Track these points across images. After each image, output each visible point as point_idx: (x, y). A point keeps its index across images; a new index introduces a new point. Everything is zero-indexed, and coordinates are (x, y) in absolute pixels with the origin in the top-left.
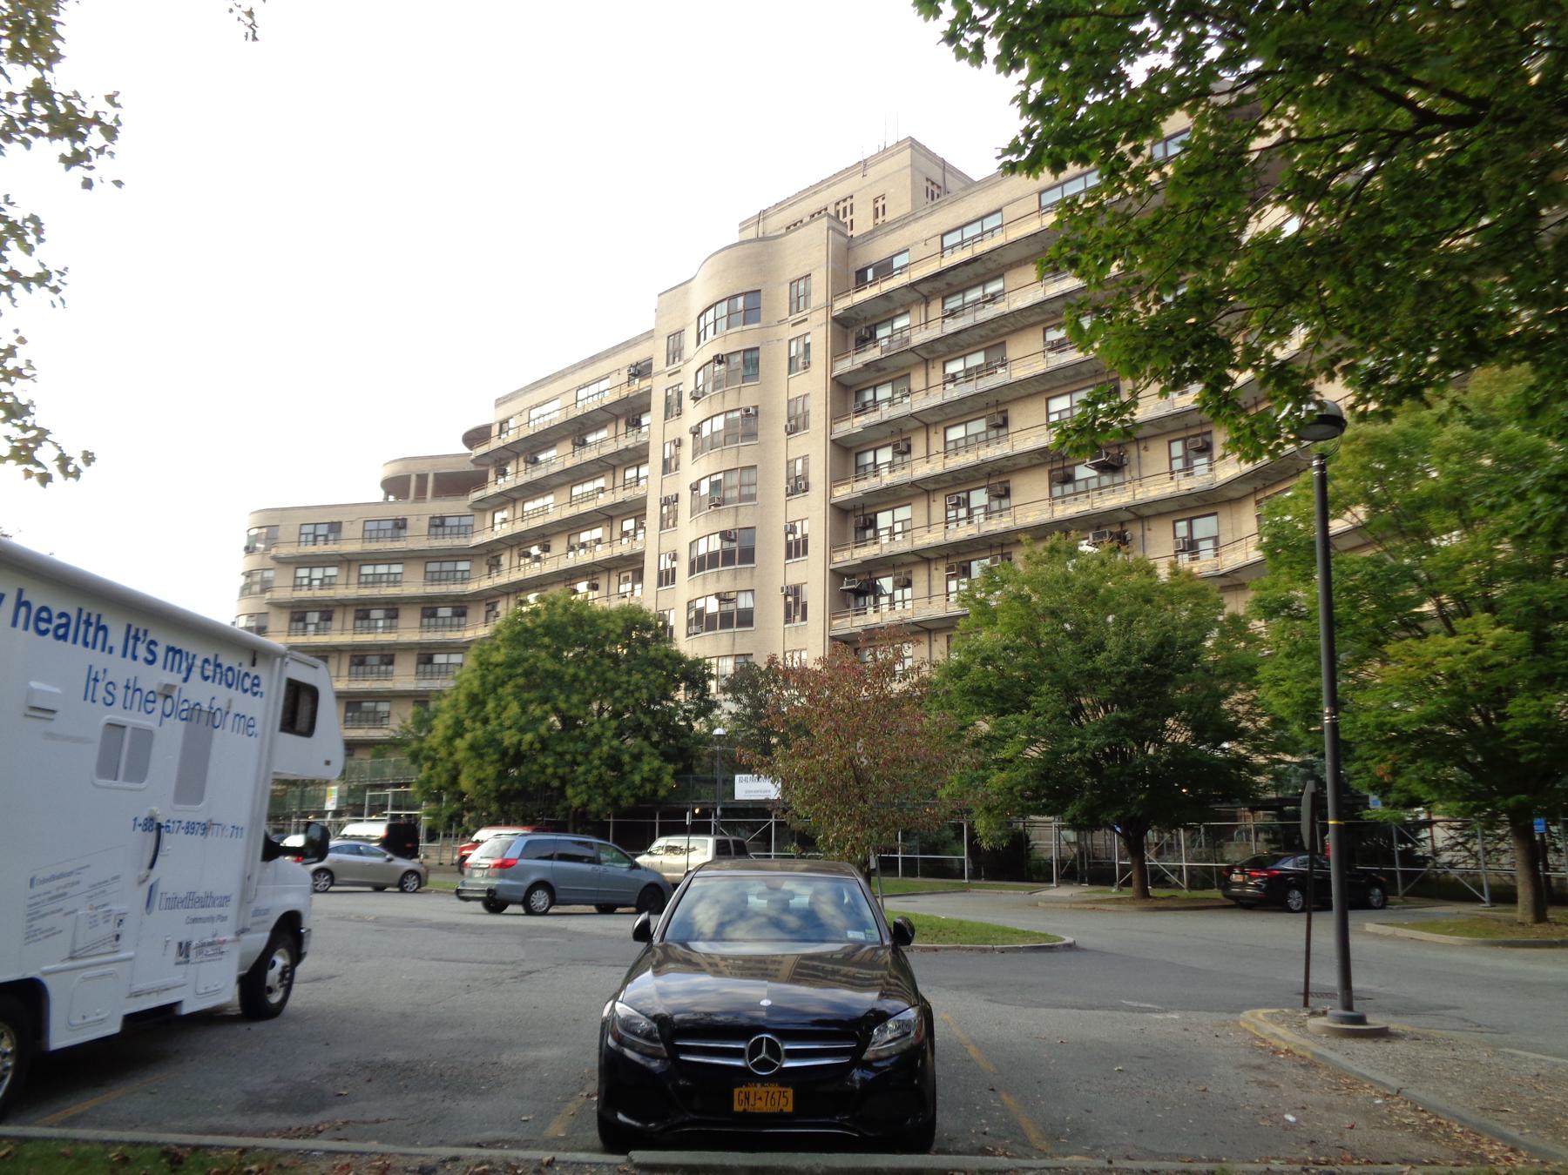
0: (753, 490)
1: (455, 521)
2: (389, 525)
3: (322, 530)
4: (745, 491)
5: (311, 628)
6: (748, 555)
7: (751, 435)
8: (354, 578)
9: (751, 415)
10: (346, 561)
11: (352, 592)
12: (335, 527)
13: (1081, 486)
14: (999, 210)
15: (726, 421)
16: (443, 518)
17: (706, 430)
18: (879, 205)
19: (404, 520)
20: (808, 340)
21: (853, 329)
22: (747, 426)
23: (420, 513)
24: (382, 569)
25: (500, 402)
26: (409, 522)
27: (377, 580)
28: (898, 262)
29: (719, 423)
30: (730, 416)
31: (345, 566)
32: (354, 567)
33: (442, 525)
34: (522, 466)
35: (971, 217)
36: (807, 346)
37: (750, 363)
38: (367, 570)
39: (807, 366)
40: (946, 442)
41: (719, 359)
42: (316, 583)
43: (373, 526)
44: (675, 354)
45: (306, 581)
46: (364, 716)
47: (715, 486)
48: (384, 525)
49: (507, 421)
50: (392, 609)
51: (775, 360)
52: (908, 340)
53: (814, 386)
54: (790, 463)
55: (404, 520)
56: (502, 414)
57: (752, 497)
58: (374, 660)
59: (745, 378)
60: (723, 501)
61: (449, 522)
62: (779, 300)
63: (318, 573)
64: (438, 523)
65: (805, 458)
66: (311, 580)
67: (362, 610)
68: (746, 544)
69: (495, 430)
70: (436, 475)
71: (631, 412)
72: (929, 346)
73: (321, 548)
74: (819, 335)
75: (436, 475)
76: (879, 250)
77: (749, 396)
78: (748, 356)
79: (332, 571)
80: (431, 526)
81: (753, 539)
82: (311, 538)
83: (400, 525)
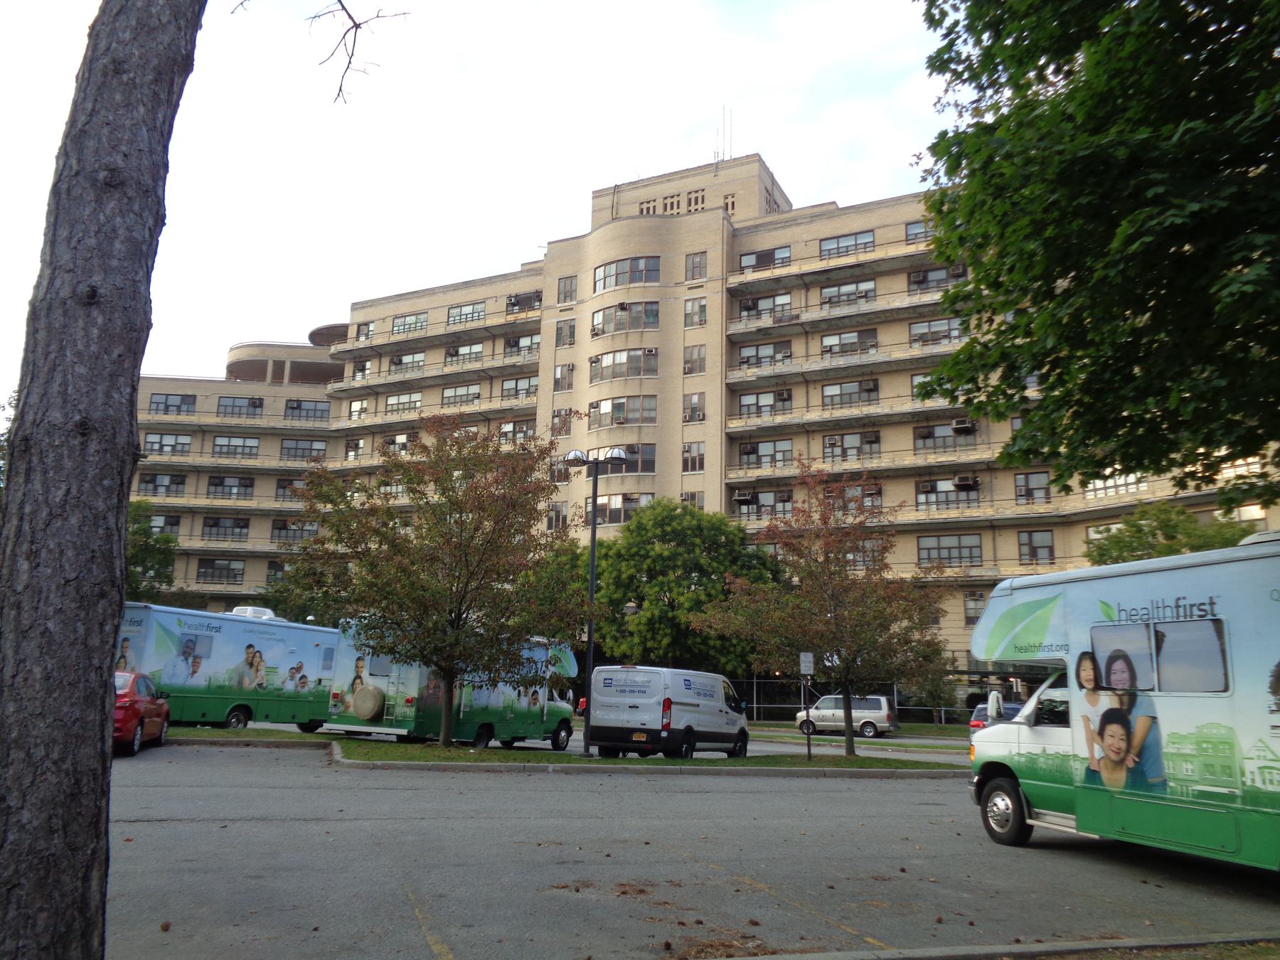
0: (653, 414)
1: (312, 406)
2: (245, 403)
3: (177, 401)
4: (646, 414)
5: (162, 490)
6: (649, 466)
7: (653, 371)
8: (208, 447)
9: (651, 354)
10: (201, 431)
11: (207, 460)
12: (189, 401)
13: (939, 442)
14: (872, 231)
15: (629, 358)
16: (299, 402)
17: (607, 361)
18: (730, 201)
19: (261, 400)
20: (703, 302)
21: (743, 299)
22: (646, 363)
23: (276, 395)
24: (237, 442)
25: (356, 307)
26: (266, 402)
27: (232, 452)
28: (779, 255)
29: (622, 358)
30: (633, 353)
31: (200, 436)
32: (209, 437)
33: (299, 407)
34: (385, 366)
35: (846, 231)
36: (703, 308)
37: (651, 313)
38: (222, 441)
39: (703, 322)
40: (823, 397)
41: (622, 307)
42: (167, 449)
43: (230, 402)
44: (568, 291)
45: (156, 447)
46: (217, 573)
47: (617, 407)
48: (238, 402)
49: (367, 324)
50: (248, 479)
51: (674, 312)
52: (798, 317)
53: (711, 338)
54: (686, 397)
55: (261, 400)
56: (361, 317)
57: (653, 420)
58: (229, 523)
59: (646, 325)
60: (627, 421)
61: (304, 405)
62: (677, 266)
63: (169, 440)
64: (294, 407)
65: (702, 395)
66: (162, 446)
67: (217, 478)
68: (648, 457)
69: (352, 332)
70: (293, 363)
71: (511, 336)
72: (814, 324)
73: (171, 418)
74: (716, 303)
75: (293, 363)
76: (765, 242)
77: (650, 339)
78: (649, 307)
79: (184, 439)
80: (287, 407)
81: (653, 452)
82: (162, 407)
83: (256, 404)
